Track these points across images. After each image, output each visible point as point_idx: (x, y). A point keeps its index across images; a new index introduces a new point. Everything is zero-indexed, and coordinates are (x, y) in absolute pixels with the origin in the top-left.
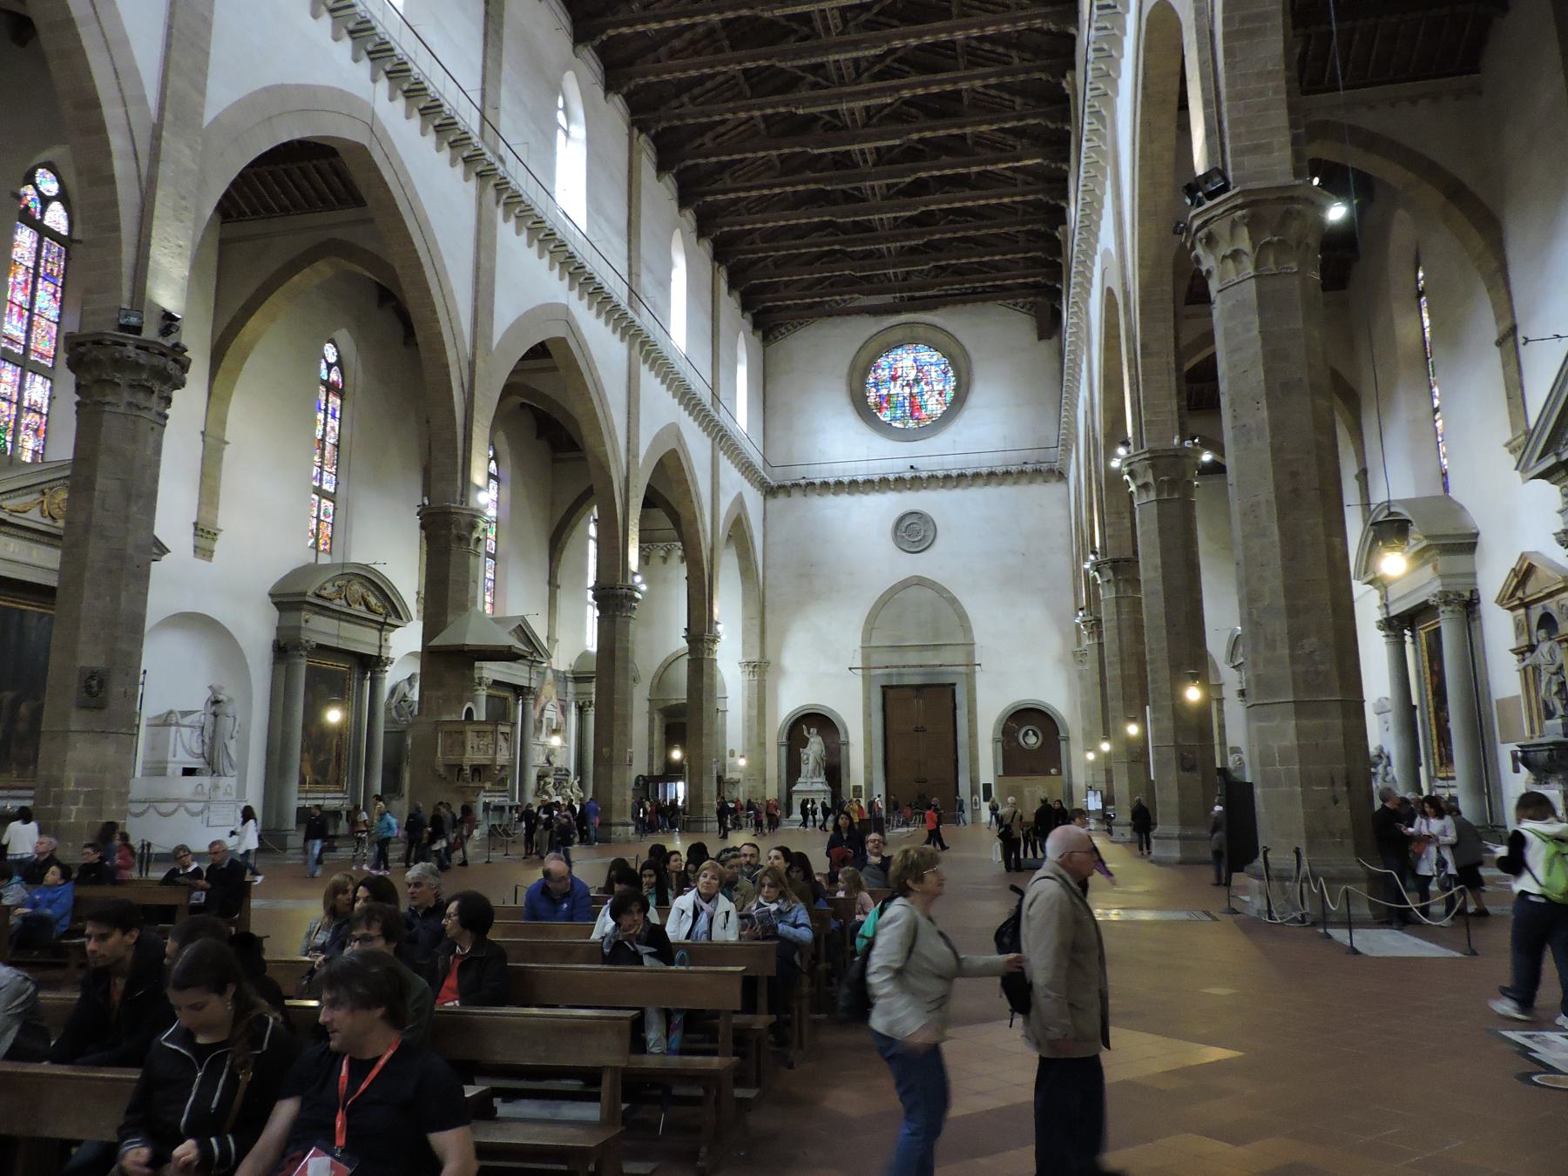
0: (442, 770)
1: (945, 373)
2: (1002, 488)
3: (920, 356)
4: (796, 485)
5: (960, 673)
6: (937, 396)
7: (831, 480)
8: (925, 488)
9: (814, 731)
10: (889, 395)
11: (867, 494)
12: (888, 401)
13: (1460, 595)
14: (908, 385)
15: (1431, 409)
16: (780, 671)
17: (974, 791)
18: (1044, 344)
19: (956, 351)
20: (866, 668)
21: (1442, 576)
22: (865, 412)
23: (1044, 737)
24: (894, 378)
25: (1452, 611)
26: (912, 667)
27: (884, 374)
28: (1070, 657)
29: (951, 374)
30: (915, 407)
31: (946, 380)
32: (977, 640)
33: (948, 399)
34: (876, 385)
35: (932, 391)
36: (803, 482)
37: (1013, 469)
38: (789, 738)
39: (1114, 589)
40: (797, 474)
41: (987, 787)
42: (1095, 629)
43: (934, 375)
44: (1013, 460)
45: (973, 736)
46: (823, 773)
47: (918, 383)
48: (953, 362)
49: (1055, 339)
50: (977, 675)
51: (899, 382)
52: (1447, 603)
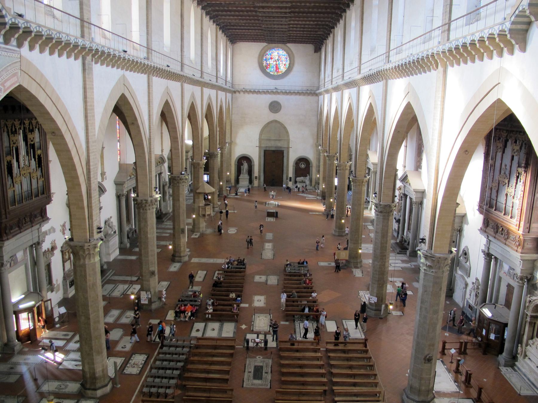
0: (201, 215)
9: (245, 162)
10: (270, 64)
17: (287, 179)
18: (316, 54)
19: (290, 53)
22: (263, 69)
24: (271, 58)
26: (273, 145)
27: (269, 57)
30: (277, 68)
31: (286, 61)
34: (266, 60)
36: (244, 90)
37: (304, 92)
38: (238, 162)
40: (241, 87)
41: (290, 178)
43: (283, 59)
49: (319, 53)
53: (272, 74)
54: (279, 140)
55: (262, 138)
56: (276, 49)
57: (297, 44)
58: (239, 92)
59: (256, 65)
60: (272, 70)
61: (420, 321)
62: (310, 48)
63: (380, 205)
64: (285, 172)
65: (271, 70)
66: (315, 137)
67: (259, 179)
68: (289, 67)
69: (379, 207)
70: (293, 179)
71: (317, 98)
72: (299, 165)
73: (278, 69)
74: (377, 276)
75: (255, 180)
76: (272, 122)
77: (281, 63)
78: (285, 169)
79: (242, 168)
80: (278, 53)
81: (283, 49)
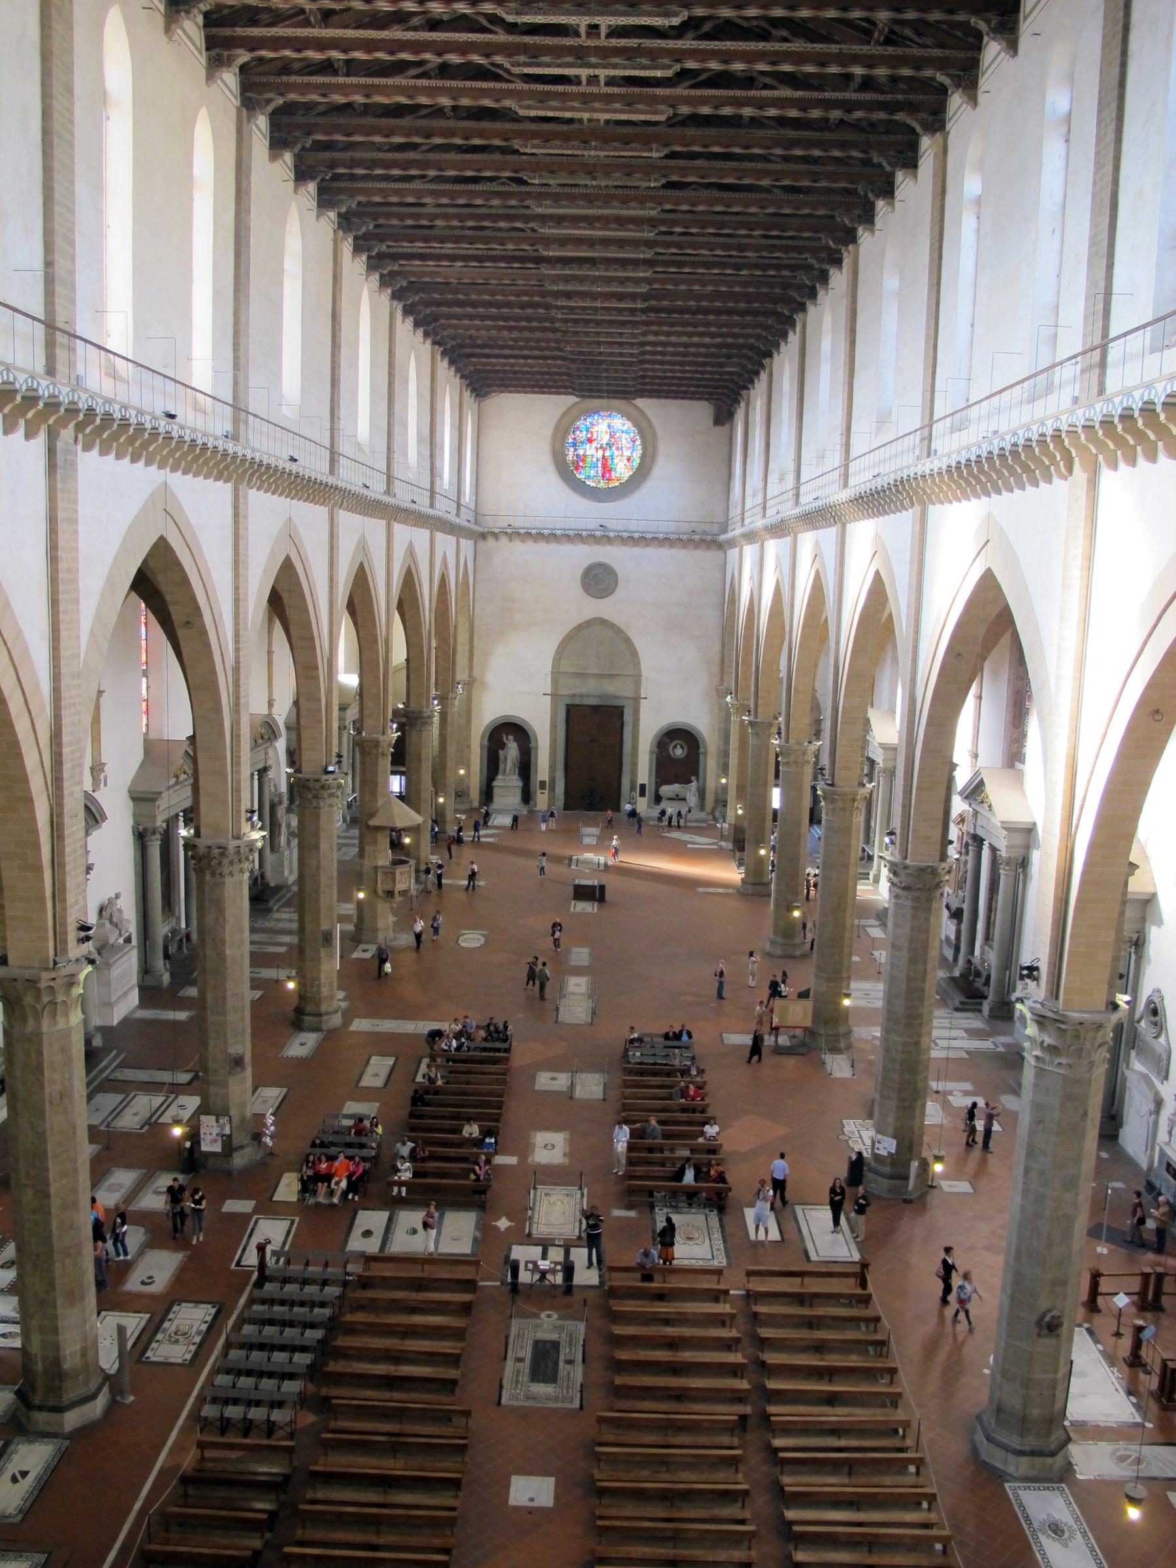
0: (380, 892)
1: (634, 442)
9: (511, 738)
10: (585, 455)
17: (633, 789)
18: (719, 429)
20: (554, 696)
22: (567, 471)
23: (689, 749)
24: (590, 441)
26: (591, 691)
28: (714, 693)
29: (638, 442)
30: (607, 469)
32: (643, 673)
34: (574, 445)
35: (622, 455)
36: (509, 531)
37: (684, 537)
40: (503, 522)
41: (643, 787)
43: (624, 442)
45: (635, 747)
48: (641, 432)
49: (727, 426)
51: (594, 444)
53: (593, 484)
54: (613, 676)
55: (562, 669)
57: (663, 401)
58: (496, 536)
59: (546, 459)
60: (593, 473)
61: (1023, 1209)
62: (702, 411)
63: (906, 867)
64: (626, 768)
65: (590, 475)
66: (716, 668)
67: (552, 789)
68: (641, 464)
69: (902, 873)
71: (720, 554)
72: (667, 751)
73: (610, 471)
74: (896, 1077)
75: (539, 791)
76: (589, 623)
77: (617, 453)
78: (626, 759)
79: (502, 757)
80: (609, 426)
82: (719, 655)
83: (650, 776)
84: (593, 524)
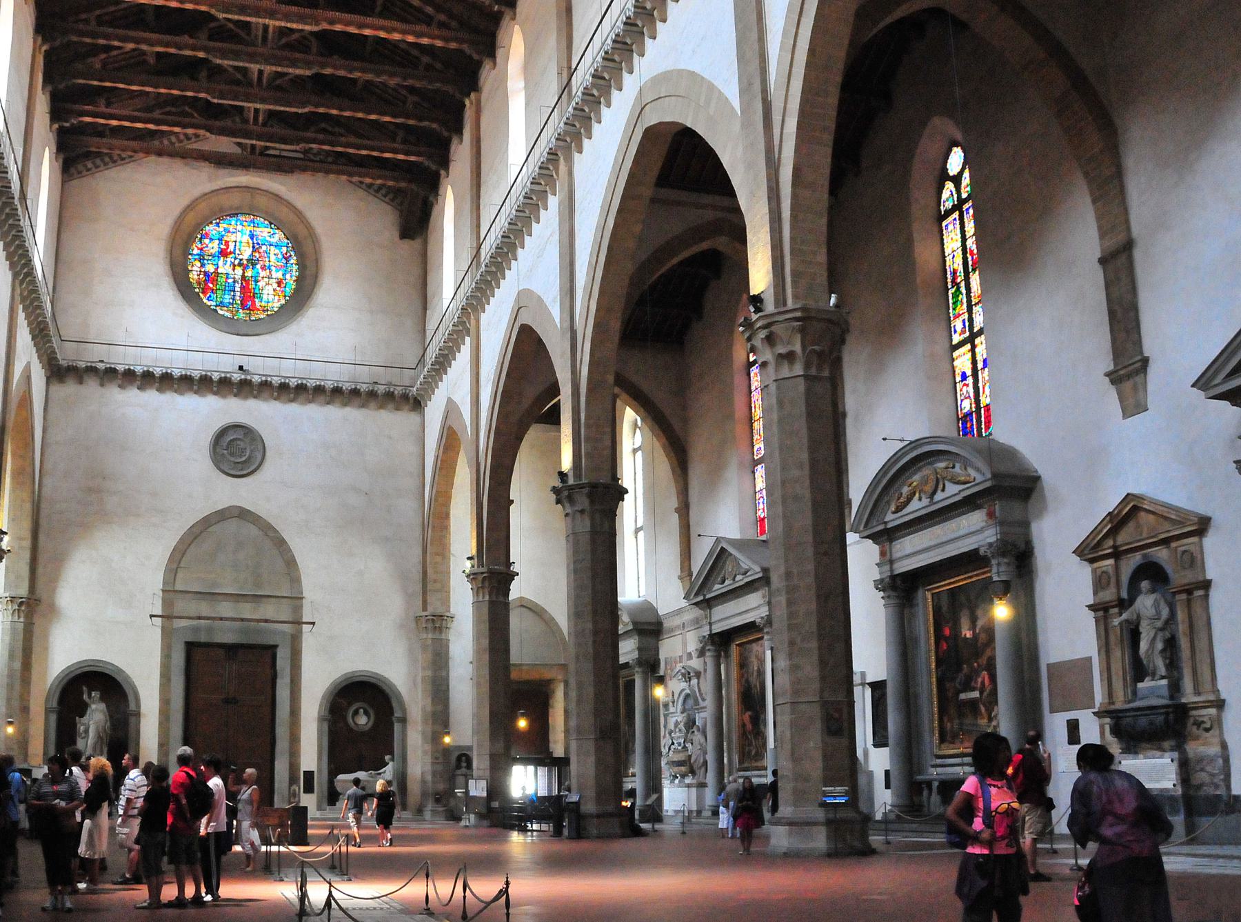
1: (287, 259)
2: (348, 410)
3: (257, 231)
4: (92, 370)
5: (284, 633)
6: (275, 286)
7: (139, 369)
8: (255, 397)
10: (217, 273)
11: (182, 394)
12: (214, 281)
13: (1015, 546)
14: (240, 265)
15: (947, 345)
16: (53, 611)
17: (293, 780)
19: (302, 231)
21: (1002, 523)
22: (188, 292)
23: (376, 714)
24: (224, 253)
25: (1008, 564)
27: (214, 247)
29: (293, 260)
33: (288, 291)
34: (201, 259)
36: (101, 366)
38: (61, 701)
39: (588, 522)
41: (309, 776)
42: (487, 584)
43: (273, 258)
44: (363, 377)
46: (105, 750)
47: (254, 265)
50: (305, 636)
51: (230, 259)
52: (1003, 555)
56: (242, 218)
59: (158, 268)
60: (227, 299)
64: (282, 745)
68: (296, 291)
70: (320, 782)
72: (345, 719)
78: (282, 731)
80: (252, 237)
81: (276, 223)
82: (420, 568)
83: (320, 759)
84: (222, 365)
